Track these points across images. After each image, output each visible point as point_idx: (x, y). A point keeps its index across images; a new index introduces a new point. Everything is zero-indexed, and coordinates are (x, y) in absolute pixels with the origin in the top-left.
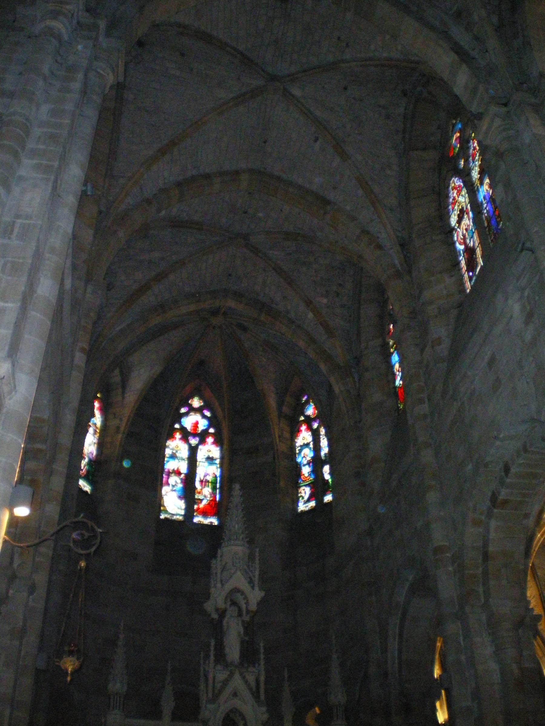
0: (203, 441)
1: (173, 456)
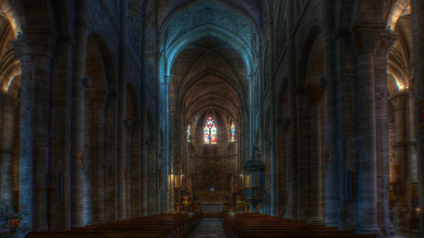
0: (212, 127)
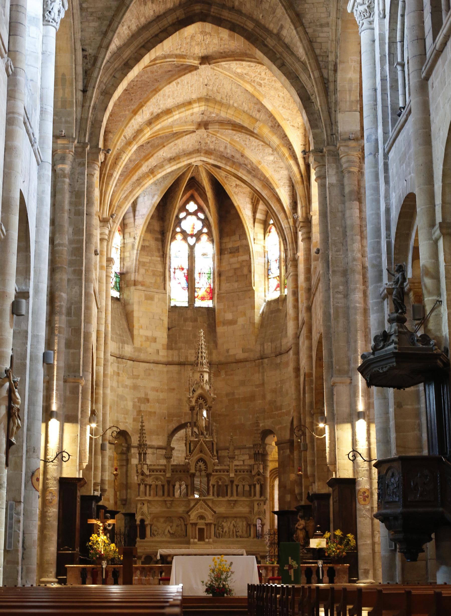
0: (198, 239)
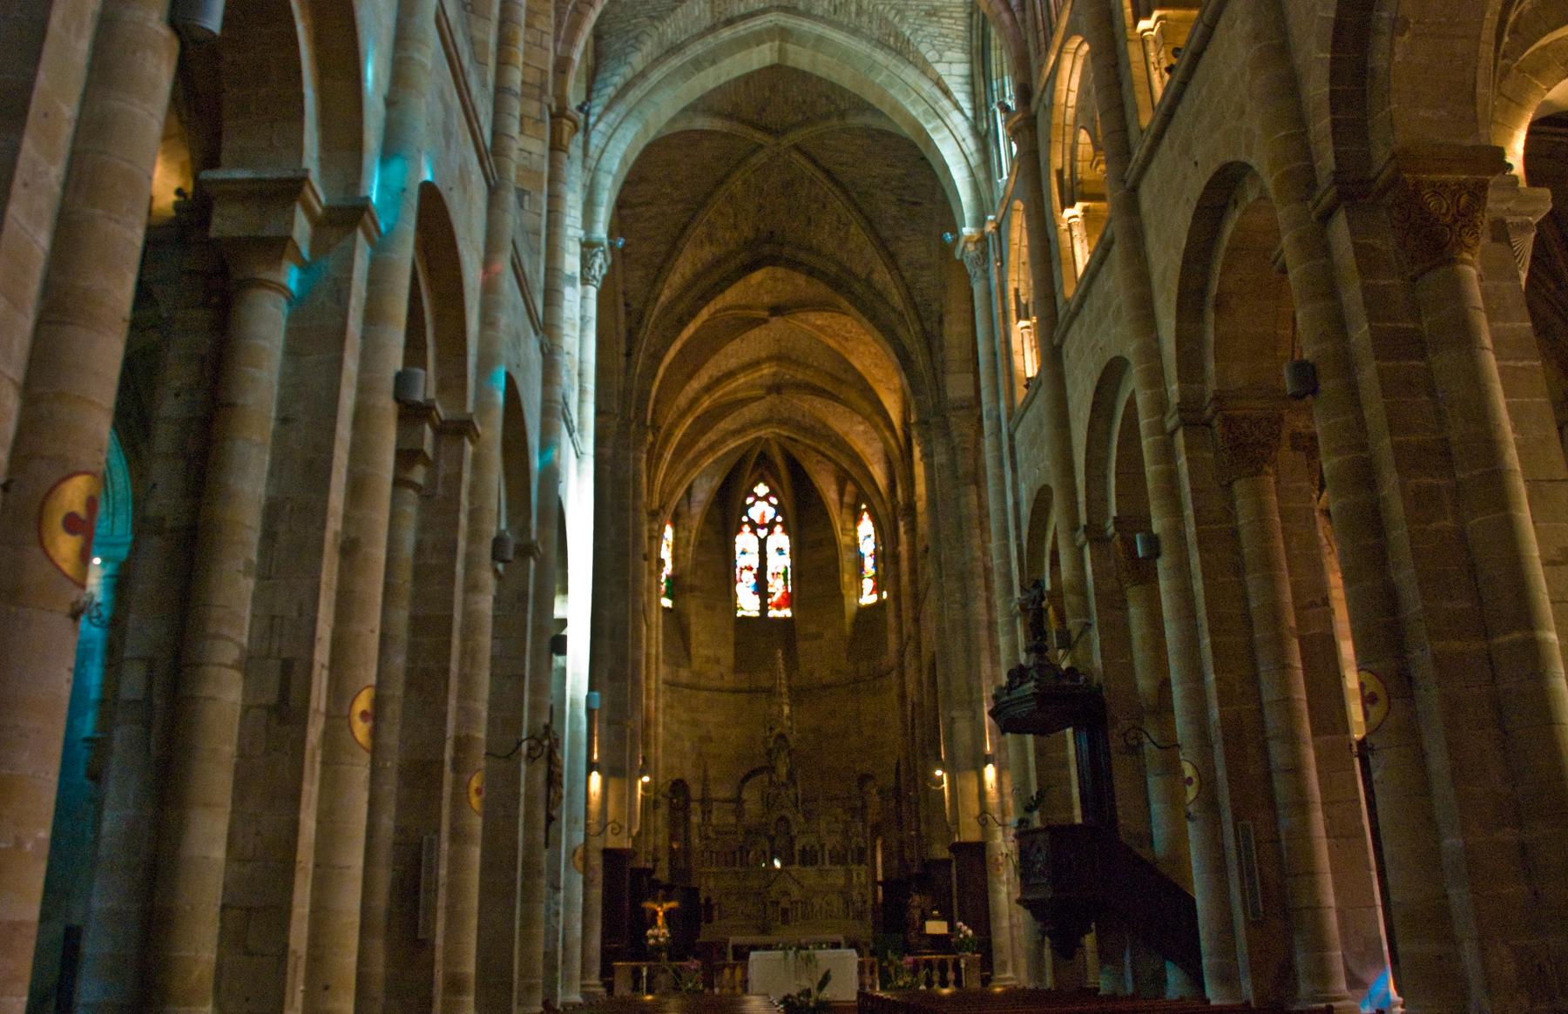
0: (771, 532)
1: (743, 553)
